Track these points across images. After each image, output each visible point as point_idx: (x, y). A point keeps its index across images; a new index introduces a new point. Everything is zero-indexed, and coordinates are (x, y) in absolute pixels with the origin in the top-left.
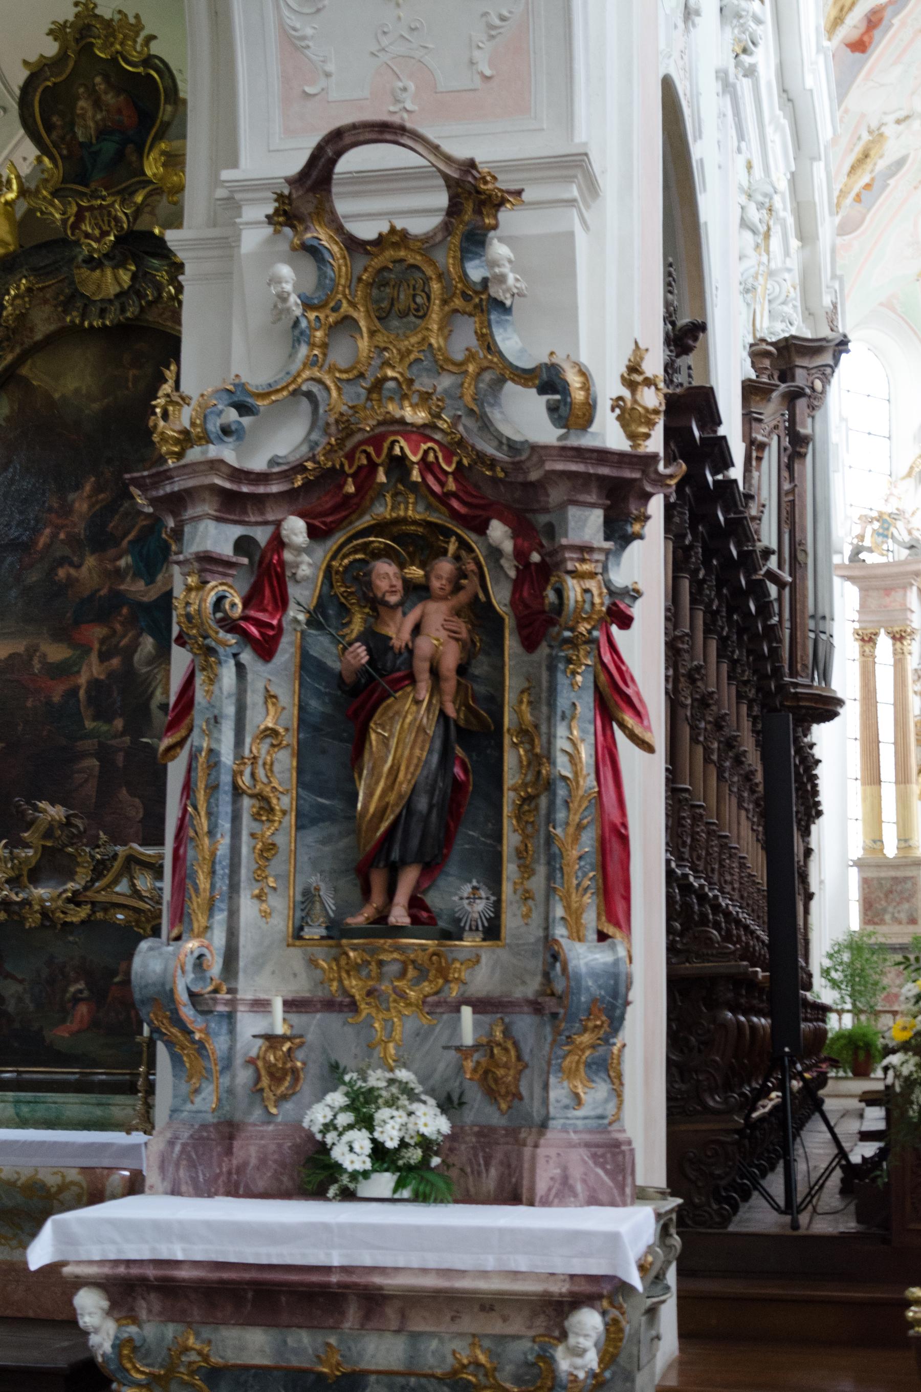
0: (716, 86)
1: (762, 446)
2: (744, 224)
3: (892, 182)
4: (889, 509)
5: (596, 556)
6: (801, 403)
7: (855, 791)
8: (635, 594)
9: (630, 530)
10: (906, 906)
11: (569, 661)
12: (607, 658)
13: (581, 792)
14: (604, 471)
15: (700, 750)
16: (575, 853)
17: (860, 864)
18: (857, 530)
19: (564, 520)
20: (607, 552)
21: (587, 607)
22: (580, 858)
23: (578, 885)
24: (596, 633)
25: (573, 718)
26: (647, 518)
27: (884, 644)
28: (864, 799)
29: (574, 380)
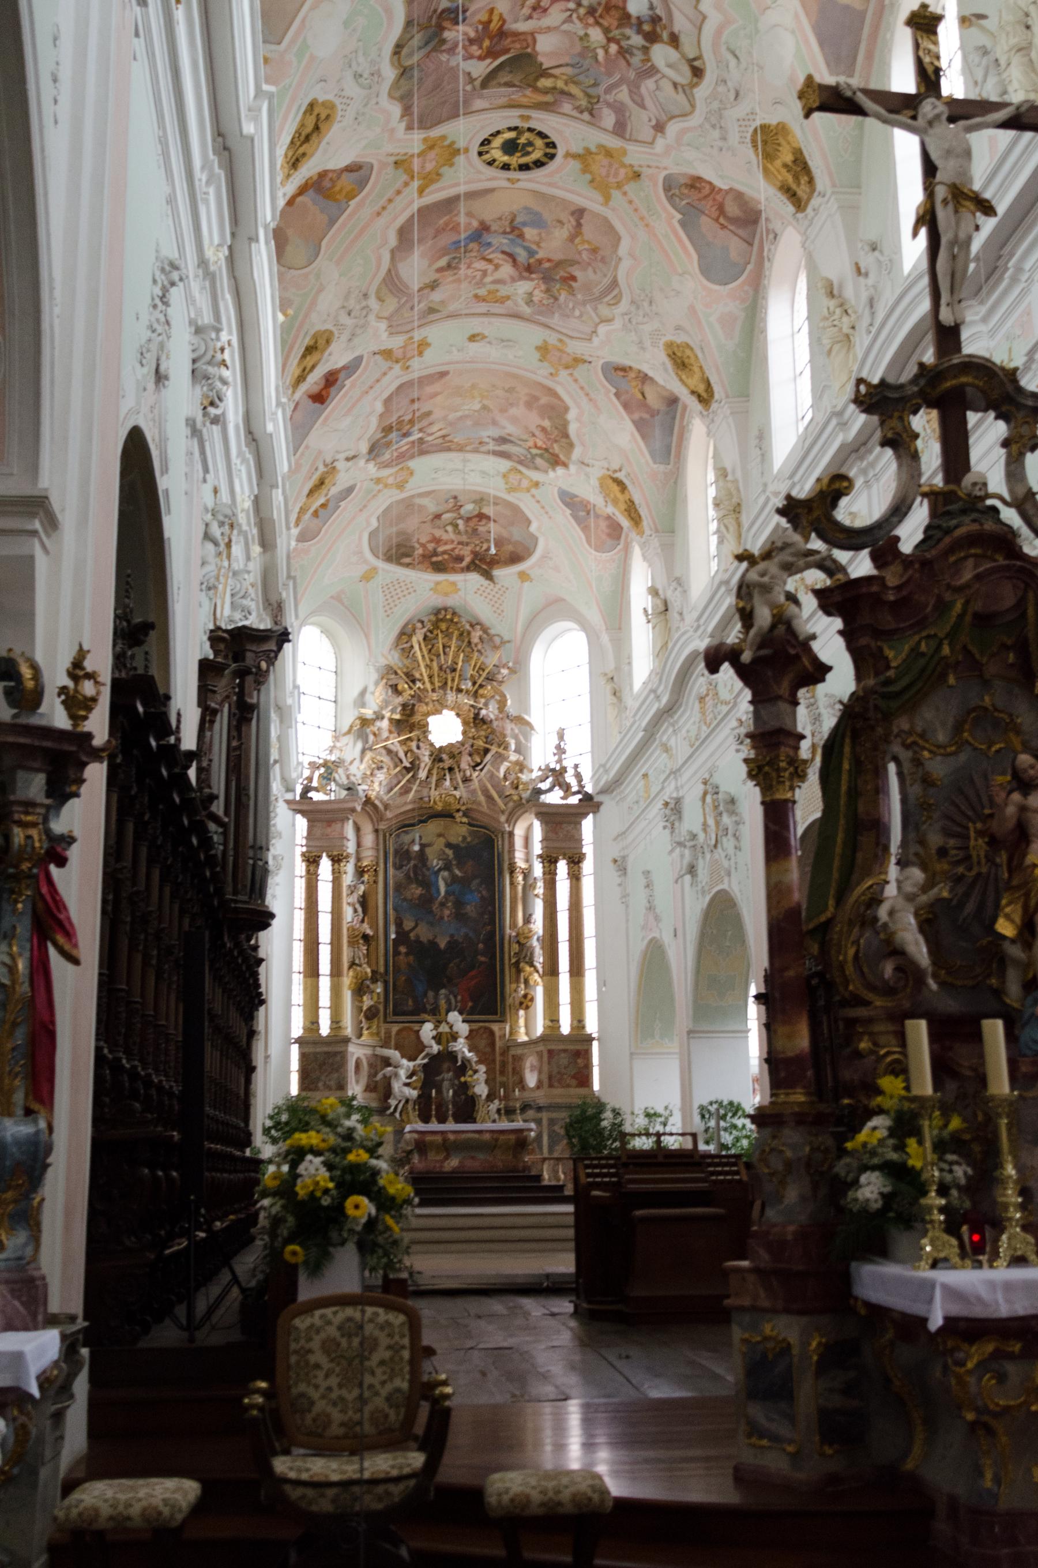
0: (185, 431)
1: (214, 712)
2: (207, 536)
3: (343, 504)
4: (333, 758)
5: (39, 810)
6: (250, 679)
7: (298, 982)
8: (69, 840)
9: (68, 790)
10: (336, 1075)
11: (13, 892)
12: (44, 890)
13: (17, 996)
14: (48, 744)
15: (139, 958)
16: (9, 1046)
17: (299, 1041)
18: (307, 773)
19: (14, 781)
20: (48, 808)
21: (29, 849)
22: (13, 1049)
23: (10, 1072)
24: (35, 871)
25: (13, 936)
26: (83, 781)
27: (325, 866)
28: (305, 989)
29: (26, 672)
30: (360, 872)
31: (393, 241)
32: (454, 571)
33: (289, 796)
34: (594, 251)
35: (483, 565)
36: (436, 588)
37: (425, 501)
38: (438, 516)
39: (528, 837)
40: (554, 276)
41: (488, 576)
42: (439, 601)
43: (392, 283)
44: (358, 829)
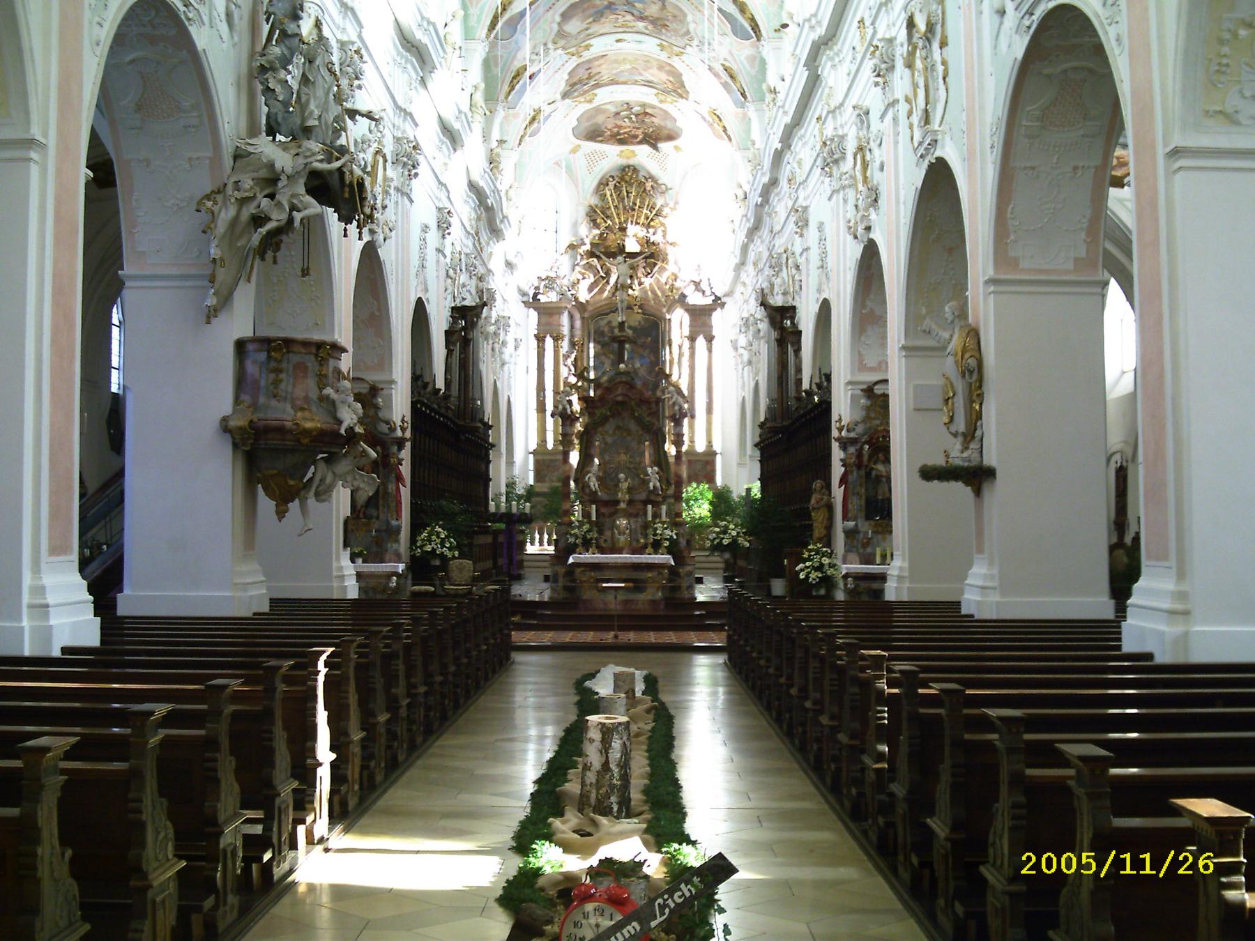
2: (448, 276)
7: (533, 415)
27: (549, 342)
30: (573, 344)
31: (558, 19)
32: (632, 143)
33: (525, 299)
34: (675, 16)
35: (653, 139)
36: (621, 154)
37: (608, 107)
38: (618, 113)
39: (679, 323)
40: (659, 24)
41: (655, 147)
42: (624, 162)
43: (561, 34)
44: (571, 317)
